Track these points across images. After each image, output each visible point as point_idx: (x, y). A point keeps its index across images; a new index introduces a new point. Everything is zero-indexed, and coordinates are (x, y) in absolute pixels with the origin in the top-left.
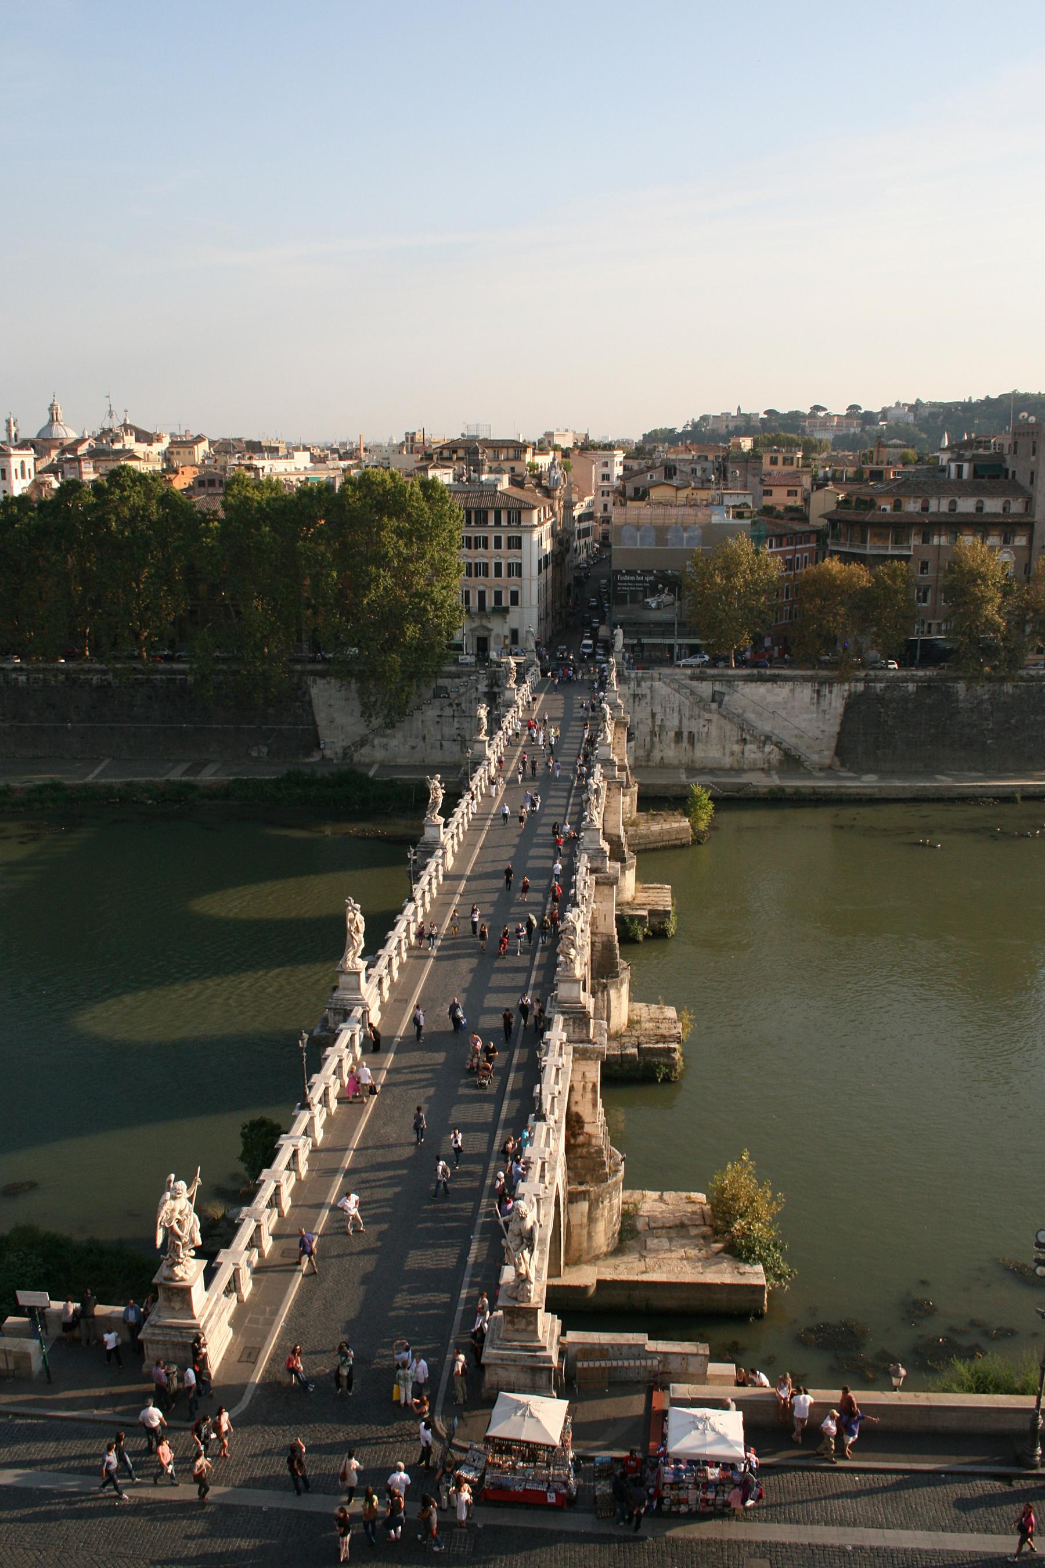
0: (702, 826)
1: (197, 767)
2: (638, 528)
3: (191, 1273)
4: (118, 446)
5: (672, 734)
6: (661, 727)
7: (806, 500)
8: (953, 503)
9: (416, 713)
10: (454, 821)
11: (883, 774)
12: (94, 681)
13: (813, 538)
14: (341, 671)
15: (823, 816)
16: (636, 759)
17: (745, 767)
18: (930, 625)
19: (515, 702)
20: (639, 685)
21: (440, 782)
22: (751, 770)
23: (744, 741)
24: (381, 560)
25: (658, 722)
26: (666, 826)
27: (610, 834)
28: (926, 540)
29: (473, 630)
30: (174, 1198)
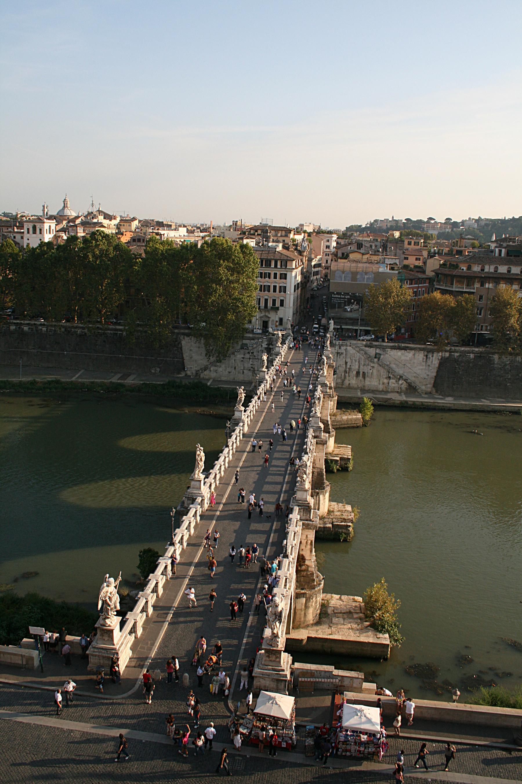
0: (367, 418)
1: (125, 376)
2: (343, 272)
3: (114, 623)
4: (95, 220)
5: (355, 373)
6: (349, 369)
7: (425, 263)
8: (496, 268)
9: (232, 356)
10: (249, 409)
11: (456, 398)
12: (78, 332)
13: (428, 281)
14: (197, 334)
15: (425, 416)
16: (337, 384)
17: (389, 390)
18: (482, 326)
19: (280, 353)
20: (340, 348)
21: (244, 390)
22: (392, 392)
23: (390, 378)
24: (219, 282)
25: (348, 367)
26: (350, 417)
28: (482, 285)
29: (261, 317)
30: (108, 586)
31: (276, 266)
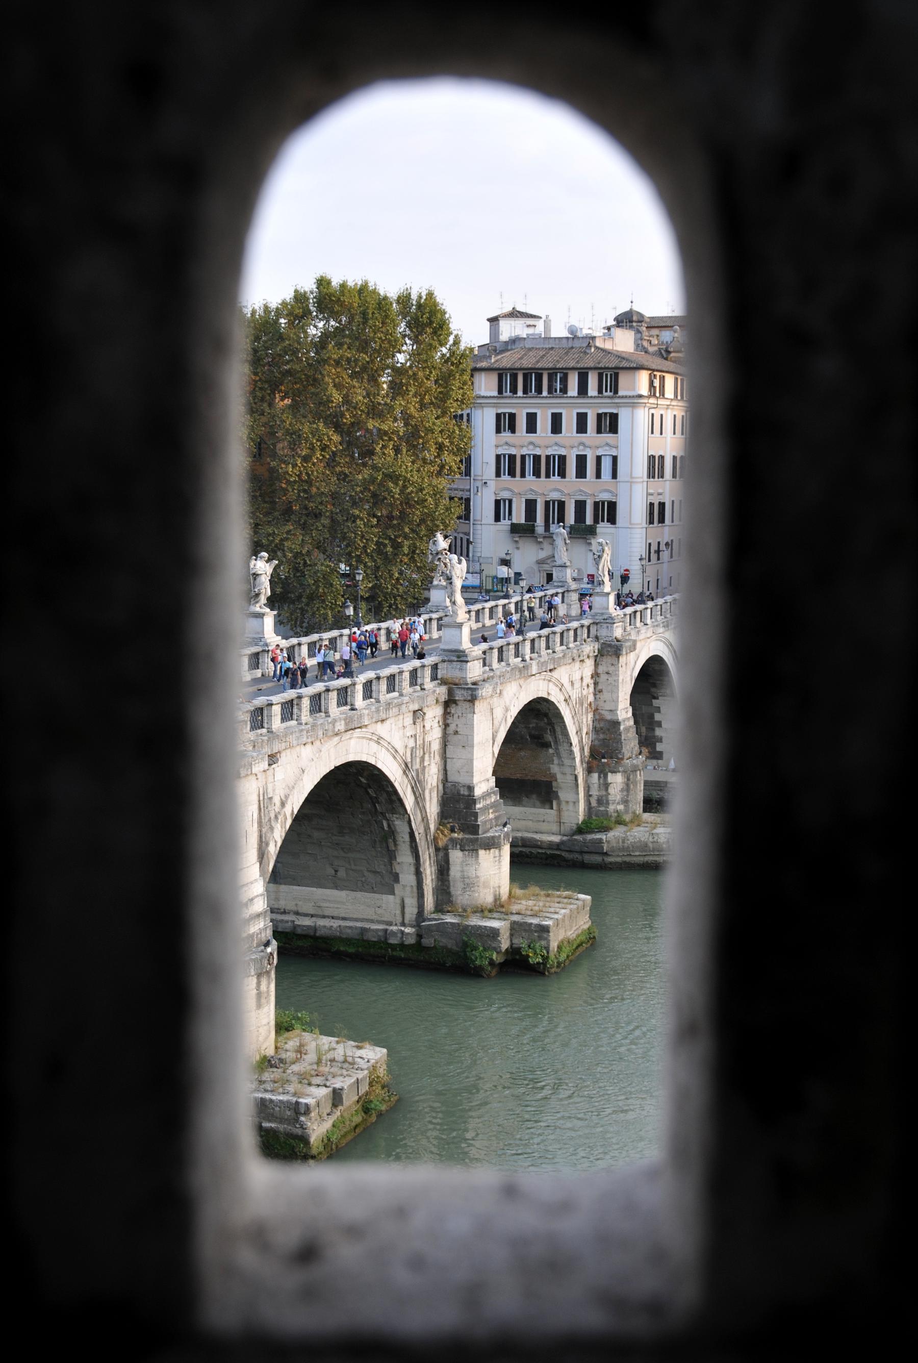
27: (455, 785)
31: (583, 389)
